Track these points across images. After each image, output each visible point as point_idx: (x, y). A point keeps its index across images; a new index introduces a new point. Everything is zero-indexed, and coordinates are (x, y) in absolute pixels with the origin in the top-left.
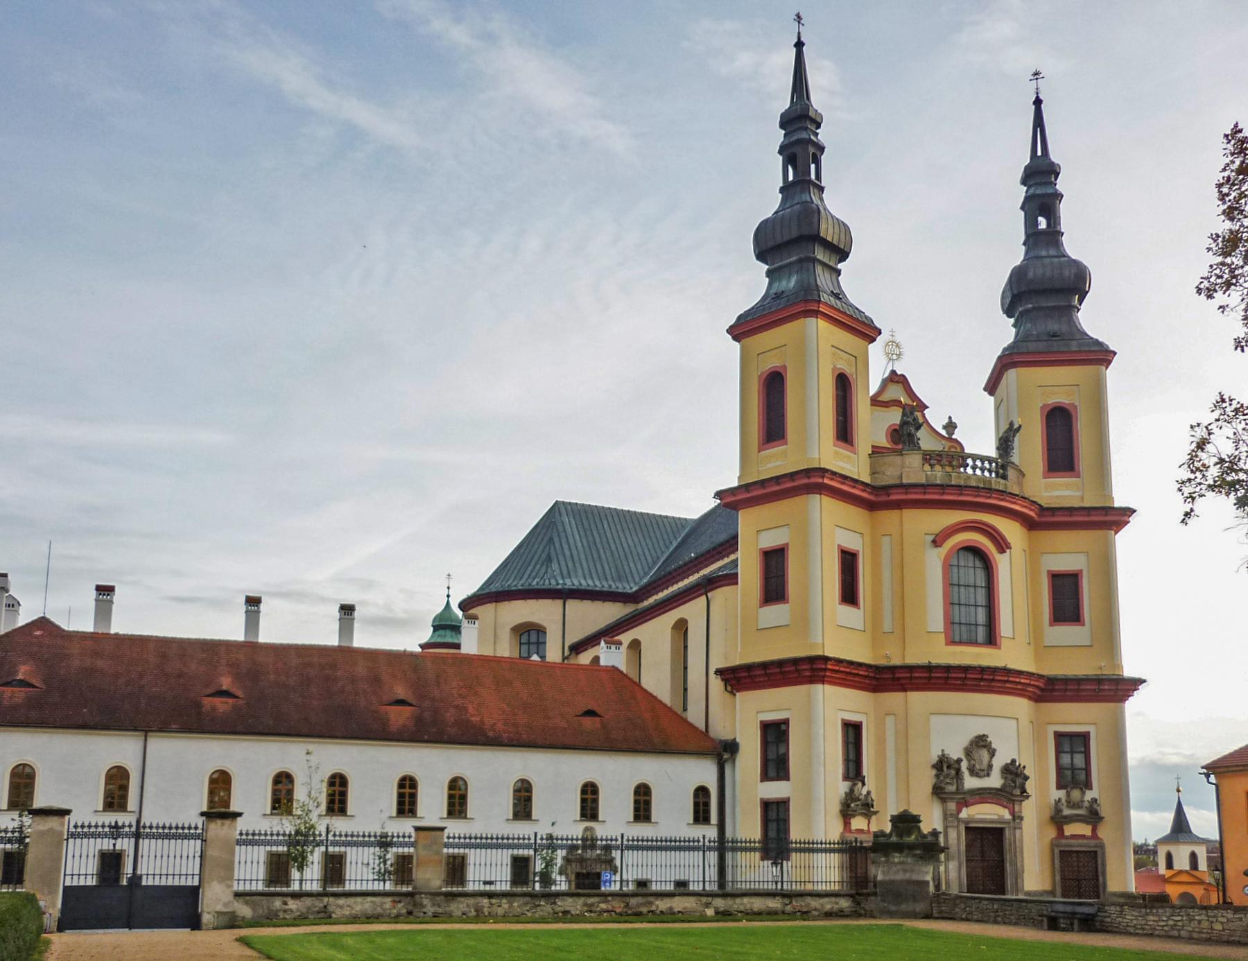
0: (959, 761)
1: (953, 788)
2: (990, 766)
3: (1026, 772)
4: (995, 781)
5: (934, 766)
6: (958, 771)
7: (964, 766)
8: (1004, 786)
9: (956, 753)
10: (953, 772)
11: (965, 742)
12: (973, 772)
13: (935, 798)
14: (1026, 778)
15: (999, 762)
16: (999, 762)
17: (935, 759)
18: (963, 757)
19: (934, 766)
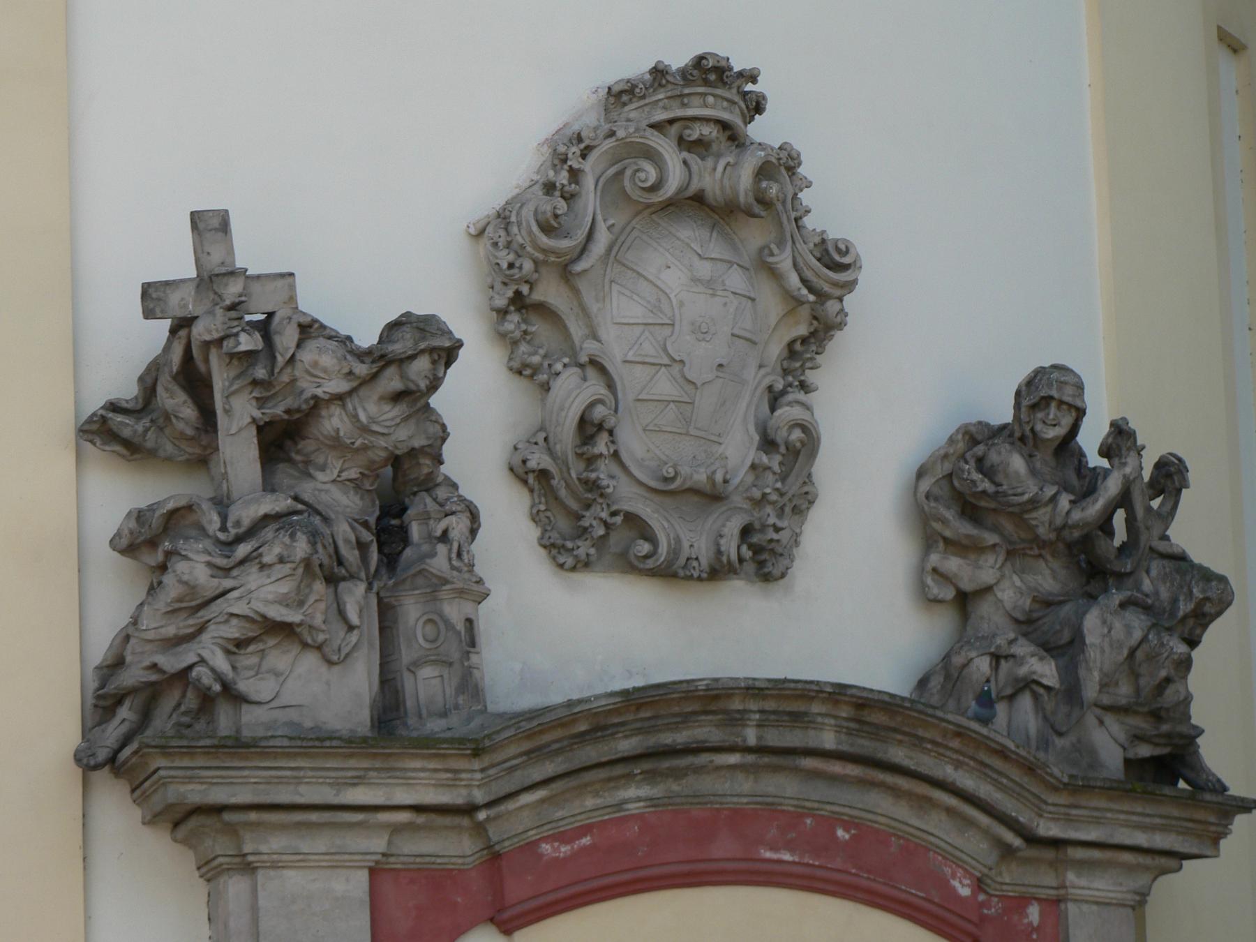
0: (417, 348)
1: (331, 691)
2: (790, 453)
3: (1194, 530)
4: (852, 608)
5: (111, 431)
6: (403, 503)
7: (480, 413)
8: (945, 675)
9: (378, 234)
10: (336, 492)
11: (498, 157)
12: (584, 515)
13: (115, 809)
14: (1196, 602)
15: (880, 421)
16: (880, 421)
17: (126, 348)
18: (464, 318)
19: (111, 431)
